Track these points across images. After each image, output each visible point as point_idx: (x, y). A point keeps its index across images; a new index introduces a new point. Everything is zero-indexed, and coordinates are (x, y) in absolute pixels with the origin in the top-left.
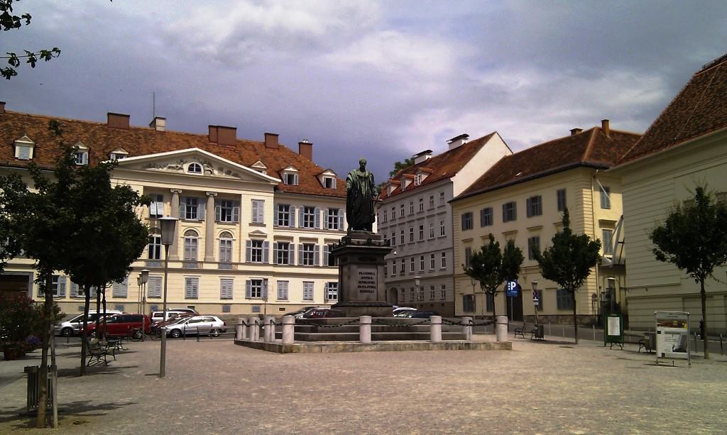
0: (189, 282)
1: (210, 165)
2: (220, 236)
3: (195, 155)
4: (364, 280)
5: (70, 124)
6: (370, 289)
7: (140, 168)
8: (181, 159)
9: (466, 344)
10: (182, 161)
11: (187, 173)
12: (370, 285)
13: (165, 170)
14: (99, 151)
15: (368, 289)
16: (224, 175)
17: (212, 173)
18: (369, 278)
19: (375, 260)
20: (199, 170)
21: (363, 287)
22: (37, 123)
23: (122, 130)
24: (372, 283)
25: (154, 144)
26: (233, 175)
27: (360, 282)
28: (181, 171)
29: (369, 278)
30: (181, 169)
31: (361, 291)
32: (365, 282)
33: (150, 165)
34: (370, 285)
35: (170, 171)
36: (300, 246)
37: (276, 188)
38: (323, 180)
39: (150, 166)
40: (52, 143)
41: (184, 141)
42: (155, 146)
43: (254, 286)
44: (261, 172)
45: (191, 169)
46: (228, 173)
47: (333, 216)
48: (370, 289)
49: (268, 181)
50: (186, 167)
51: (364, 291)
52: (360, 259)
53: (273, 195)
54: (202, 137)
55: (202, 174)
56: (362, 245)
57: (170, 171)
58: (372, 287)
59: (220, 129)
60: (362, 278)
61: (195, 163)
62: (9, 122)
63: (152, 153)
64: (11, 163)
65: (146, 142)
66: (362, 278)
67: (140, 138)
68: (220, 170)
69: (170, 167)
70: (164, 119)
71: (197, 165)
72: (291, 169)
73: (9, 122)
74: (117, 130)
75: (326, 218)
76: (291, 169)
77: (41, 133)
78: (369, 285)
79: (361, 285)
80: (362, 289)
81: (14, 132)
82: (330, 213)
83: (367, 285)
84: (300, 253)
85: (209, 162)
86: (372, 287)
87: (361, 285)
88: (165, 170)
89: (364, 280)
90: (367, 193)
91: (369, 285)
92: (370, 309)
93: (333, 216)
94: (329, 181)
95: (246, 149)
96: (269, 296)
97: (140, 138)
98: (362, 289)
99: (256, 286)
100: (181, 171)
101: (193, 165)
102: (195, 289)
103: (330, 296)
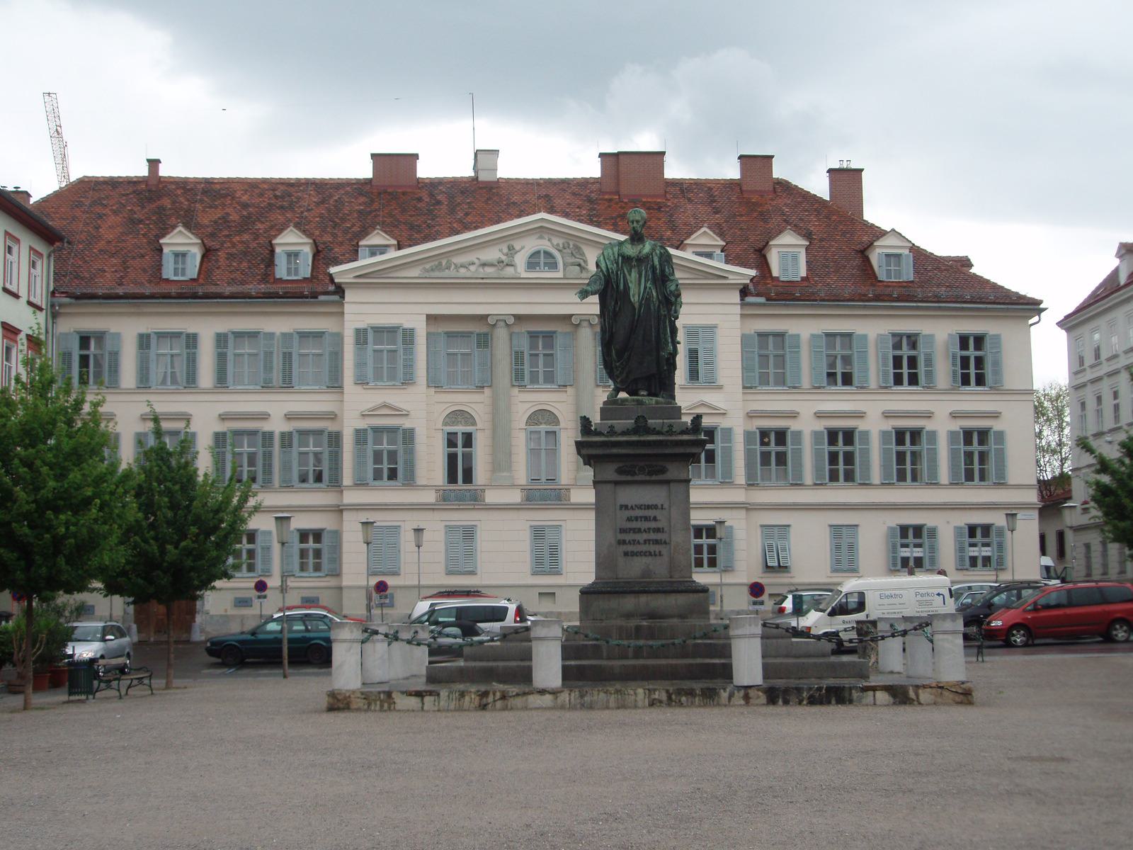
0: (538, 533)
2: (445, 424)
3: (542, 230)
4: (635, 525)
5: (292, 190)
6: (653, 548)
7: (415, 272)
9: (829, 689)
11: (524, 275)
12: (653, 536)
15: (644, 548)
18: (647, 519)
19: (663, 471)
21: (634, 542)
24: (658, 530)
25: (467, 214)
27: (623, 531)
29: (647, 519)
31: (626, 554)
32: (639, 531)
33: (440, 264)
34: (653, 536)
36: (748, 435)
40: (246, 237)
41: (539, 198)
43: (698, 541)
44: (709, 255)
45: (532, 264)
48: (653, 548)
51: (634, 554)
52: (620, 471)
53: (738, 309)
55: (560, 275)
56: (623, 433)
58: (657, 542)
59: (621, 157)
60: (629, 519)
62: (166, 202)
66: (629, 519)
67: (439, 202)
71: (547, 254)
75: (885, 358)
77: (225, 219)
78: (645, 536)
79: (628, 537)
80: (630, 548)
83: (641, 537)
86: (657, 542)
87: (628, 537)
89: (635, 525)
90: (646, 300)
91: (645, 536)
92: (643, 599)
96: (346, 568)
98: (630, 548)
99: (705, 541)
100: (509, 271)
101: (536, 254)
102: (554, 551)
103: (973, 561)
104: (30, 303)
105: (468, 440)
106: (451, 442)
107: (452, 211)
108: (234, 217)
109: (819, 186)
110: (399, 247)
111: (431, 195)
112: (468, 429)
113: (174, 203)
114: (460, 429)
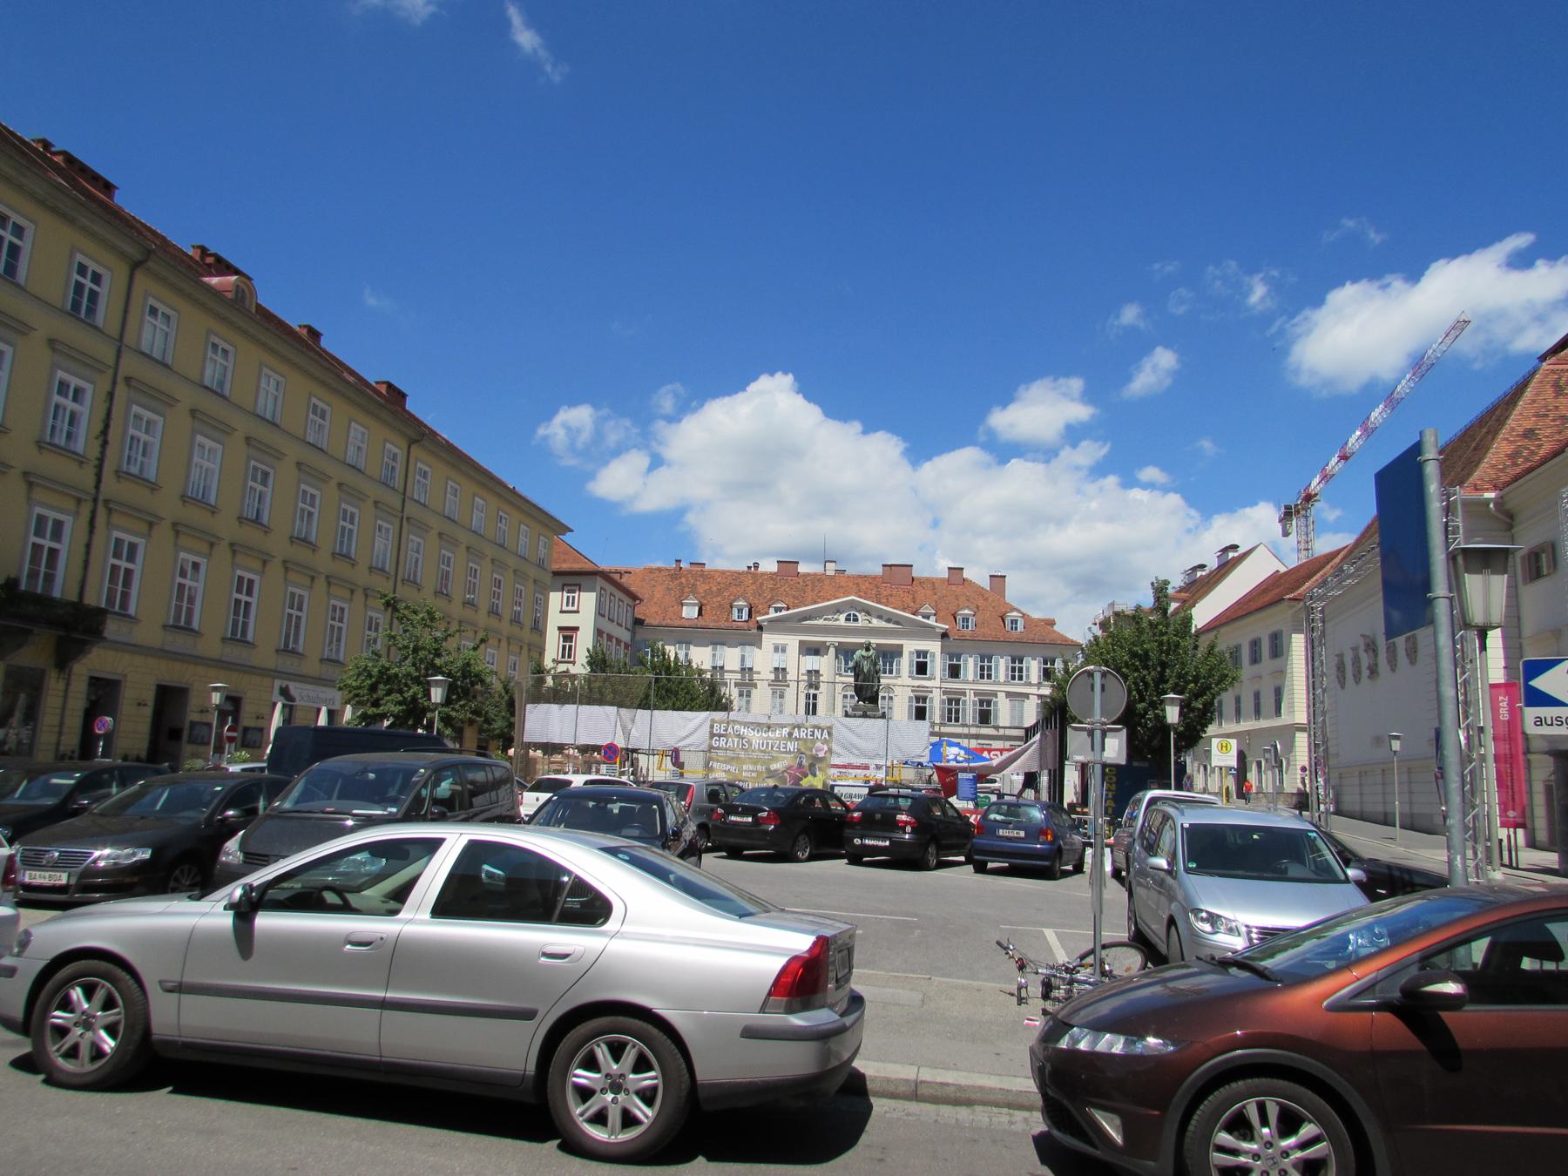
1: (868, 613)
8: (838, 610)
10: (838, 611)
11: (844, 624)
13: (821, 622)
14: (762, 604)
16: (883, 624)
17: (870, 622)
20: (856, 620)
22: (710, 578)
23: (790, 578)
26: (894, 623)
28: (837, 623)
30: (837, 620)
35: (826, 623)
37: (944, 635)
38: (1008, 621)
39: (806, 619)
41: (854, 584)
42: (821, 594)
44: (928, 618)
45: (847, 619)
46: (889, 621)
47: (1017, 665)
49: (933, 627)
50: (842, 617)
54: (875, 578)
55: (860, 625)
57: (826, 623)
61: (852, 612)
62: (683, 580)
63: (815, 603)
64: (677, 623)
65: (813, 590)
68: (880, 617)
69: (825, 619)
70: (835, 562)
71: (854, 615)
72: (966, 612)
73: (683, 580)
74: (785, 578)
76: (966, 612)
81: (687, 590)
82: (1013, 662)
84: (942, 710)
85: (868, 611)
88: (821, 622)
93: (1017, 665)
94: (1014, 622)
95: (924, 588)
97: (807, 585)
101: (849, 615)
104: (626, 628)
105: (815, 697)
106: (808, 696)
107: (813, 590)
108: (714, 589)
109: (985, 583)
110: (788, 609)
111: (804, 581)
112: (815, 692)
113: (687, 581)
114: (812, 691)
